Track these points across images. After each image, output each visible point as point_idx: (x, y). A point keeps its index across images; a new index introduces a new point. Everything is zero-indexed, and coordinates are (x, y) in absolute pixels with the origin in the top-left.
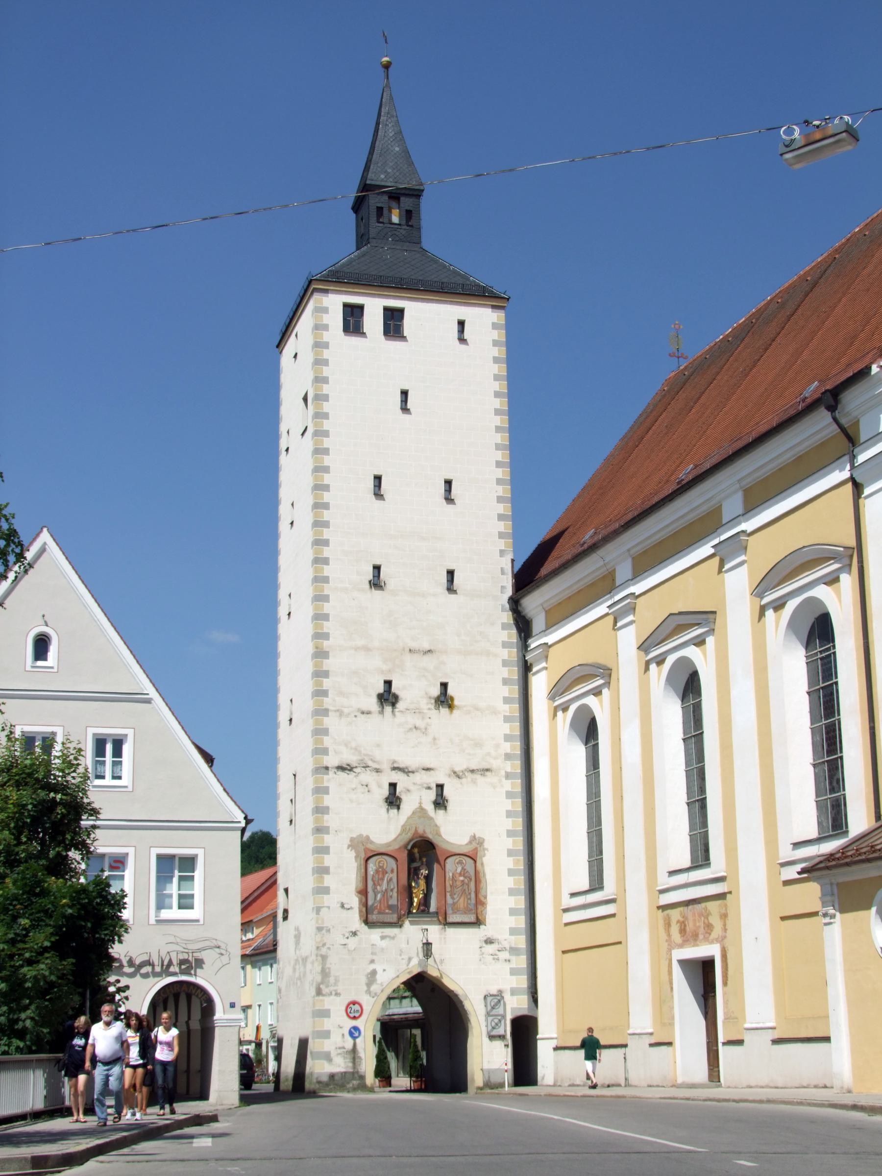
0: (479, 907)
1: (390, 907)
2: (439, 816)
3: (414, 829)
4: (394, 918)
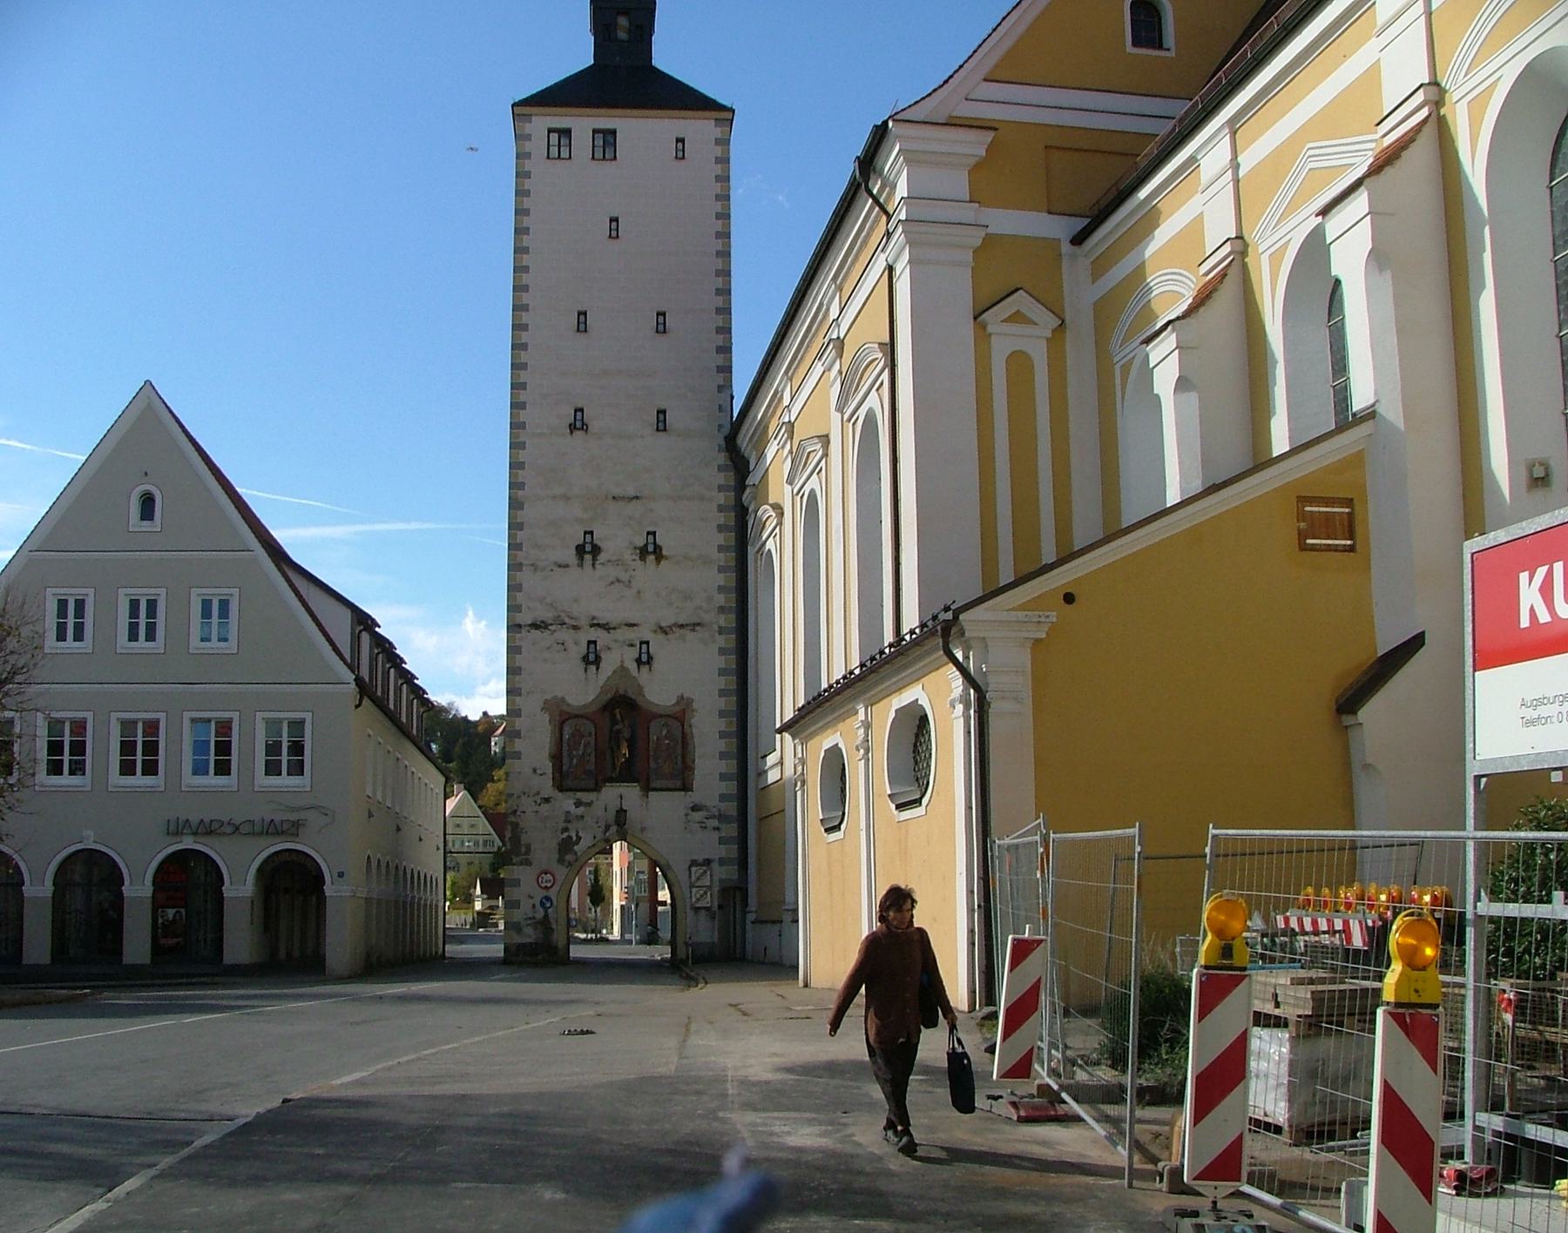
2: (643, 676)
4: (591, 785)
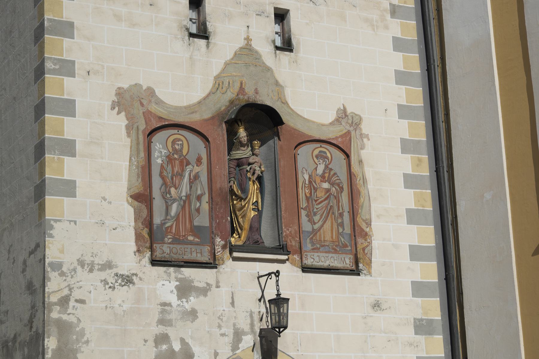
0: (360, 241)
1: (196, 231)
3: (237, 86)
